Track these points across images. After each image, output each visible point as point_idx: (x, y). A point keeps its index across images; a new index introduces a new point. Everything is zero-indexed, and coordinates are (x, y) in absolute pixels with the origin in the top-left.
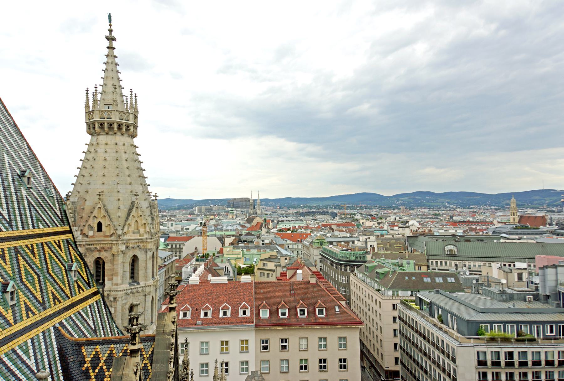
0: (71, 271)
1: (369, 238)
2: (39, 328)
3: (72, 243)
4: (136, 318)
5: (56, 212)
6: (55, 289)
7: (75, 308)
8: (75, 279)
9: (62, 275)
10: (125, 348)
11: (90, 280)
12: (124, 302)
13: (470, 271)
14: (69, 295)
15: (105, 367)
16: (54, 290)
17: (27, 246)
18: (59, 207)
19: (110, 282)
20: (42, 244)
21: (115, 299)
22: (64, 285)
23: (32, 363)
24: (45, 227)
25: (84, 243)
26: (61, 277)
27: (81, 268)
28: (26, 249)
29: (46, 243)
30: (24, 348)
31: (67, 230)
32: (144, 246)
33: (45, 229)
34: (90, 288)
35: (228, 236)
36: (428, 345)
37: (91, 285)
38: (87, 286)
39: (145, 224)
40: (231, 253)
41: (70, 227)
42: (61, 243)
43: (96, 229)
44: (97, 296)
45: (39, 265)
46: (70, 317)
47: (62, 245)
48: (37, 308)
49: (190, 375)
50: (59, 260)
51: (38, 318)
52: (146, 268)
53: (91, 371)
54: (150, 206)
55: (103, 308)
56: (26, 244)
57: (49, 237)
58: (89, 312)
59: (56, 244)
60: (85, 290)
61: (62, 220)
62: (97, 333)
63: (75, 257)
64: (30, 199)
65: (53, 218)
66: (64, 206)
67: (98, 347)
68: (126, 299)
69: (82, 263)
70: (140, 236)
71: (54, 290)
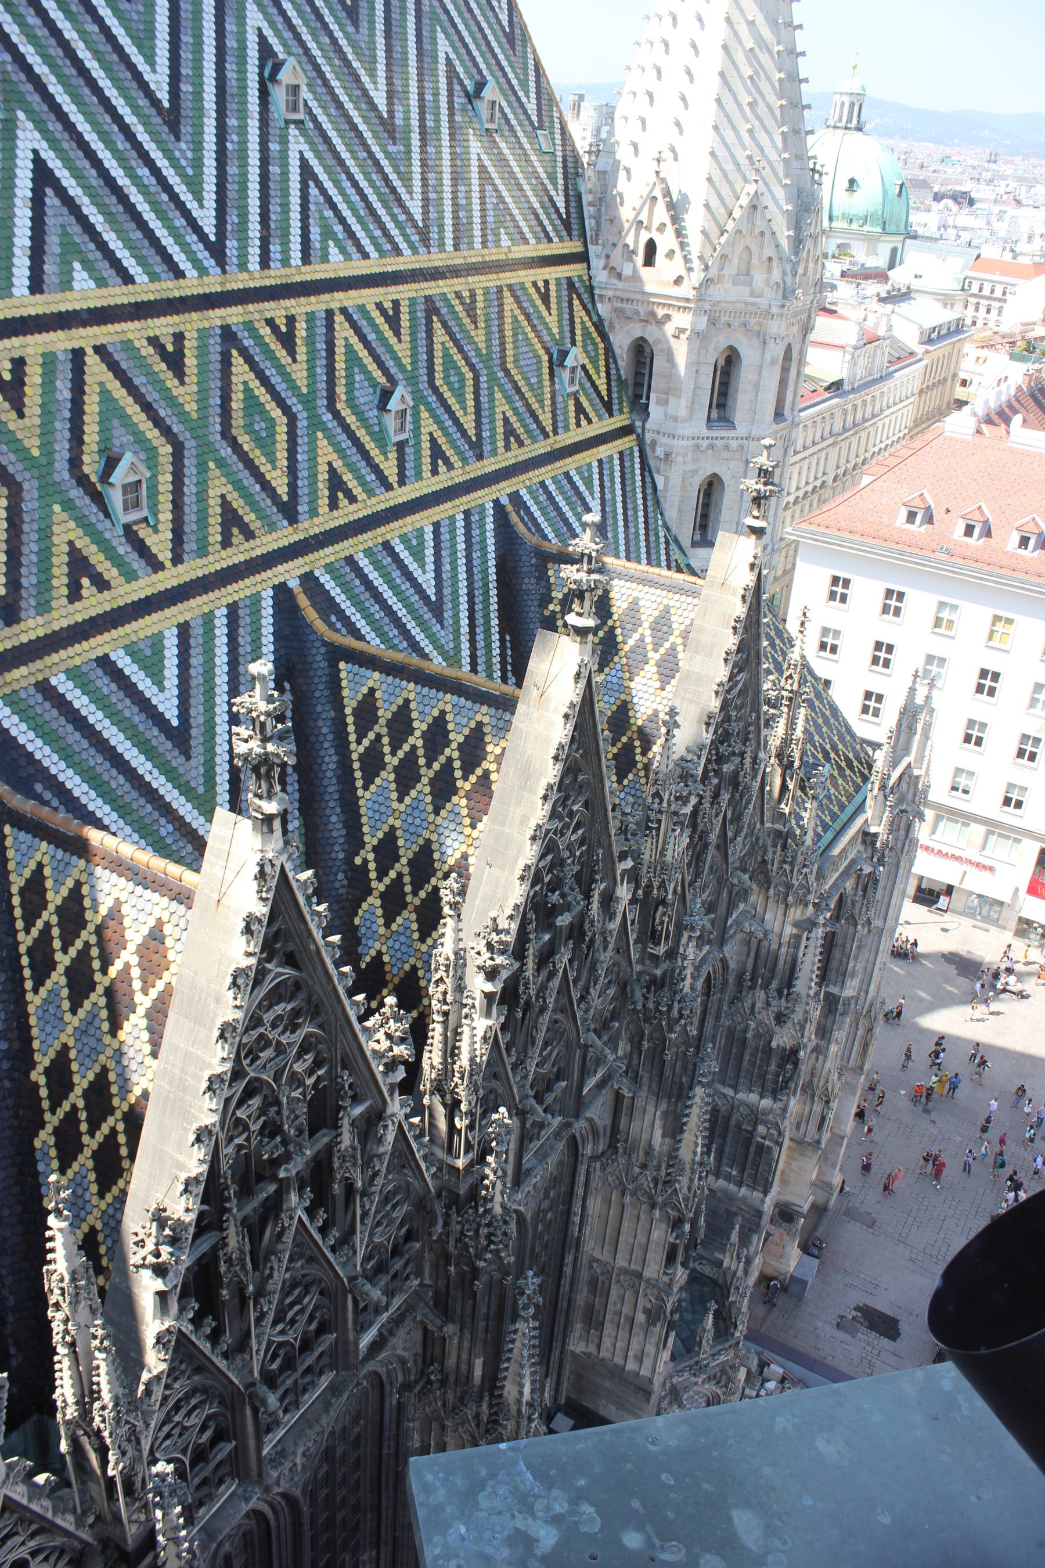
2: (457, 502)
3: (582, 290)
6: (515, 410)
7: (558, 464)
9: (539, 376)
10: (635, 594)
11: (615, 395)
12: (689, 467)
14: (549, 429)
17: (458, 295)
18: (566, 186)
19: (661, 409)
20: (500, 290)
21: (667, 455)
22: (541, 402)
23: (427, 580)
25: (610, 293)
26: (534, 380)
27: (594, 361)
28: (455, 302)
29: (510, 287)
30: (414, 542)
32: (760, 324)
34: (611, 415)
37: (615, 407)
38: (603, 411)
39: (770, 259)
42: (553, 288)
44: (626, 439)
45: (482, 346)
46: (542, 484)
47: (553, 294)
48: (460, 454)
51: (458, 476)
52: (757, 386)
55: (638, 472)
56: (458, 288)
57: (523, 273)
58: (596, 476)
60: (595, 419)
61: (567, 224)
63: (584, 328)
64: (487, 163)
65: (543, 217)
66: (580, 181)
68: (695, 460)
69: (601, 345)
70: (752, 294)
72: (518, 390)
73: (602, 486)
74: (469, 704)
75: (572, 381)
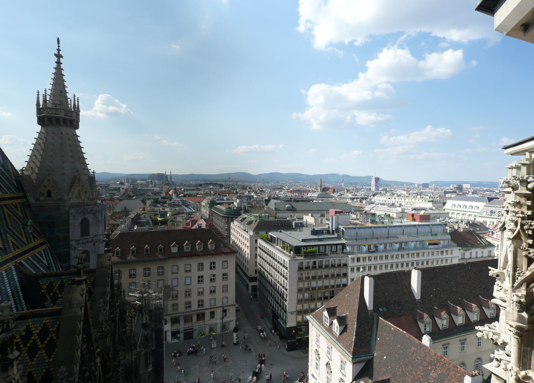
0: (27, 225)
1: (242, 201)
4: (80, 259)
5: (13, 182)
7: (31, 252)
8: (30, 232)
10: (73, 278)
13: (298, 218)
14: (26, 243)
15: (58, 292)
16: (13, 240)
24: (3, 193)
26: (18, 230)
29: (5, 205)
31: (22, 195)
33: (4, 195)
35: (149, 199)
36: (274, 261)
39: (85, 192)
40: (151, 211)
41: (24, 193)
42: (18, 205)
43: (46, 195)
46: (28, 258)
47: (18, 206)
49: (123, 292)
50: (16, 217)
53: (47, 295)
54: (89, 179)
57: (8, 201)
58: (43, 254)
59: (14, 206)
60: (39, 239)
62: (50, 268)
67: (51, 278)
71: (13, 240)
72: (14, 233)
73: (45, 256)
74: (39, 319)
75: (30, 230)
